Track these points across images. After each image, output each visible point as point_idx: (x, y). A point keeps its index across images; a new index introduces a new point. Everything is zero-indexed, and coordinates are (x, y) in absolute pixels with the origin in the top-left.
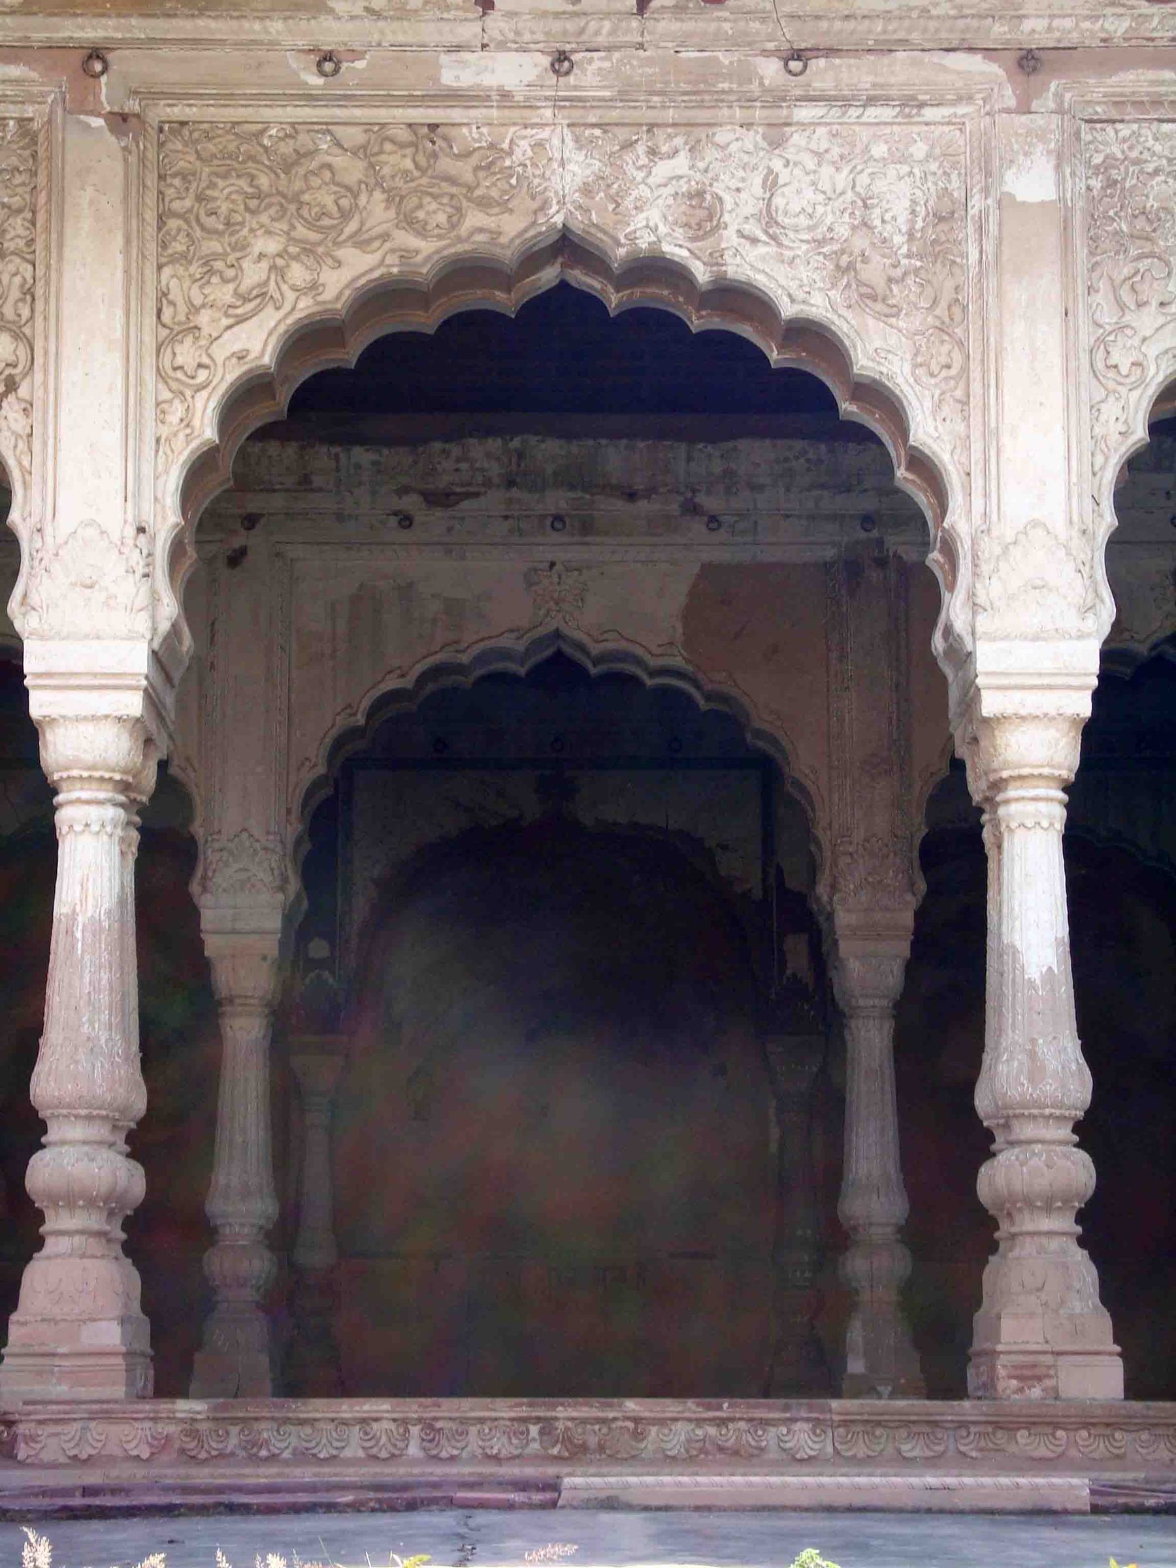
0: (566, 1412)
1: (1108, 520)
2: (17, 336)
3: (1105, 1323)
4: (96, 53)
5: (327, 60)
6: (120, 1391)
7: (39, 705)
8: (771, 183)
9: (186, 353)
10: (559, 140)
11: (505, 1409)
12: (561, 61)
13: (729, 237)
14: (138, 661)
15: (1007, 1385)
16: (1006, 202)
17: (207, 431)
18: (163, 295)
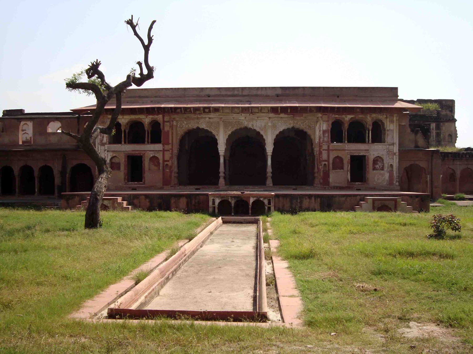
0: (246, 187)
1: (273, 142)
2: (218, 132)
3: (272, 182)
4: (221, 118)
5: (233, 118)
6: (224, 185)
7: (219, 152)
8: (256, 124)
9: (226, 133)
10: (245, 121)
11: (243, 186)
12: (245, 118)
13: (254, 127)
14: (224, 150)
15: (267, 185)
16: (269, 126)
17: (227, 137)
18: (225, 130)
